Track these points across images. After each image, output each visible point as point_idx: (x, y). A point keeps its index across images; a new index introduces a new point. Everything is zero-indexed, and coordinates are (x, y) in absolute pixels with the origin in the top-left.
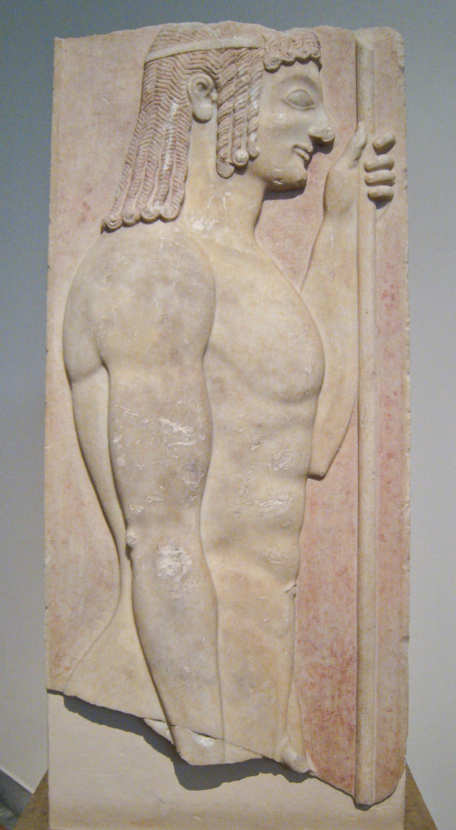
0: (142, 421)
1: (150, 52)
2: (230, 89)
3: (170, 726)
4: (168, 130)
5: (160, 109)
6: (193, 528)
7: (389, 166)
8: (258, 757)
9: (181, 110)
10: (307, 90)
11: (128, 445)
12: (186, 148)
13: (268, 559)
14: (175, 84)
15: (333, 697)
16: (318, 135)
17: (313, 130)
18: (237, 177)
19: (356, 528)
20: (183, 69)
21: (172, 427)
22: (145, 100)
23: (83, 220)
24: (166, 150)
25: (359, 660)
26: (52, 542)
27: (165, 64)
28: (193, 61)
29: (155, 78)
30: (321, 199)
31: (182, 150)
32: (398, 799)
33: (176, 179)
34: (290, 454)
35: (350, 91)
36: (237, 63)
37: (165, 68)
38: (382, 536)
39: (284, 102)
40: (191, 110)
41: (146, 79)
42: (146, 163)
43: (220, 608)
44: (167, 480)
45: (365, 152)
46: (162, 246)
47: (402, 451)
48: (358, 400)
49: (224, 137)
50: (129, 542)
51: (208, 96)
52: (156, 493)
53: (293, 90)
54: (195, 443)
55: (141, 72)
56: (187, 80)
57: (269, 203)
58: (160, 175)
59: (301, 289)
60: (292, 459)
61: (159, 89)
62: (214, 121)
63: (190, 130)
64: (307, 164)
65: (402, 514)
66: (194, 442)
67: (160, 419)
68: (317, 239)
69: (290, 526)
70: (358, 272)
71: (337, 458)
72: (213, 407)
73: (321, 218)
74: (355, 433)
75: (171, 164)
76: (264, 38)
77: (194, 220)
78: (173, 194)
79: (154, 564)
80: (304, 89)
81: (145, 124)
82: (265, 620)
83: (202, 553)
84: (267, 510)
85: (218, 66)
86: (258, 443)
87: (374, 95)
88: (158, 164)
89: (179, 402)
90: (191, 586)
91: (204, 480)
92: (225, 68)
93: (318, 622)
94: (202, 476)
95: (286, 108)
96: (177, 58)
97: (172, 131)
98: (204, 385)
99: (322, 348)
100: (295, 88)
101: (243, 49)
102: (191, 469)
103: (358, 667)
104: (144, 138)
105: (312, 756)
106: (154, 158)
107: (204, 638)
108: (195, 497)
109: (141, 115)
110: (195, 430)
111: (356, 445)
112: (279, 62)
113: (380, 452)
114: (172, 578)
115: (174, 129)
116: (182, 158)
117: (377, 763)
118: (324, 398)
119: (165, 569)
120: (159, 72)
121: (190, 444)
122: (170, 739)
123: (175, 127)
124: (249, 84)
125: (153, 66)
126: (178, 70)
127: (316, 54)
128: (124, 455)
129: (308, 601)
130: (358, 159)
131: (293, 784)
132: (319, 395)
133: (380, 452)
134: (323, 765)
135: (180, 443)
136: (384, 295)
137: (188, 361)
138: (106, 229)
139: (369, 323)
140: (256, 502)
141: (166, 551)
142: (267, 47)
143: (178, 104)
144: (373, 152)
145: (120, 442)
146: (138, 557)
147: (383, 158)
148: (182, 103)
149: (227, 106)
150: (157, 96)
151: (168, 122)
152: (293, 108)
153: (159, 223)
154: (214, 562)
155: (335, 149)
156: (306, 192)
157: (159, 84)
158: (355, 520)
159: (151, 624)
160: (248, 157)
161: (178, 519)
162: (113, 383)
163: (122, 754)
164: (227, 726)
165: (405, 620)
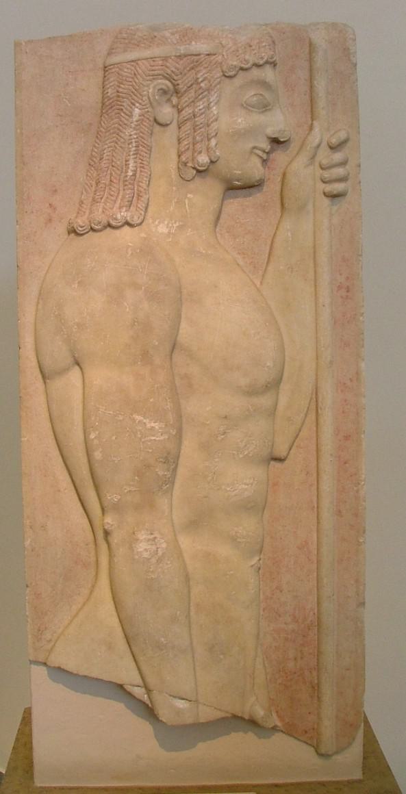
0: (116, 418)
1: (109, 54)
3: (149, 691)
4: (131, 135)
5: (123, 114)
6: (166, 514)
7: (343, 163)
8: (229, 715)
9: (143, 115)
17: (270, 131)
18: (198, 181)
19: (316, 506)
20: (144, 76)
21: (145, 423)
22: (107, 104)
24: (129, 155)
26: (31, 527)
27: (126, 70)
28: (154, 68)
32: (356, 749)
33: (141, 184)
34: (254, 442)
36: (197, 69)
38: (340, 512)
41: (107, 83)
42: (111, 167)
43: (191, 583)
46: (130, 253)
48: (317, 389)
50: (106, 527)
51: (169, 100)
52: (131, 483)
53: (250, 95)
54: (167, 437)
55: (101, 73)
56: (148, 86)
59: (261, 283)
61: (121, 94)
62: (174, 126)
63: (151, 134)
64: (264, 161)
65: (357, 491)
73: (279, 214)
75: (135, 168)
77: (159, 223)
78: (138, 199)
79: (131, 548)
80: (261, 93)
81: (107, 128)
86: (224, 433)
88: (122, 168)
89: (151, 400)
91: (175, 470)
92: (185, 74)
93: (281, 591)
94: (173, 467)
96: (137, 64)
97: (135, 137)
101: (202, 56)
102: (164, 461)
103: (318, 631)
104: (107, 142)
105: (277, 712)
107: (178, 613)
110: (166, 425)
111: (315, 429)
112: (237, 69)
113: (337, 435)
114: (148, 559)
115: (136, 134)
116: (145, 162)
117: (337, 717)
118: (285, 387)
119: (141, 552)
121: (162, 438)
122: (148, 702)
124: (209, 90)
125: (113, 70)
126: (139, 76)
128: (101, 450)
130: (313, 157)
136: (340, 288)
138: (73, 231)
139: (326, 314)
140: (223, 487)
141: (142, 536)
142: (224, 53)
143: (140, 109)
144: (329, 150)
145: (95, 438)
147: (338, 157)
149: (187, 112)
153: (126, 228)
154: (185, 542)
157: (121, 90)
158: (315, 499)
160: (209, 161)
162: (86, 381)
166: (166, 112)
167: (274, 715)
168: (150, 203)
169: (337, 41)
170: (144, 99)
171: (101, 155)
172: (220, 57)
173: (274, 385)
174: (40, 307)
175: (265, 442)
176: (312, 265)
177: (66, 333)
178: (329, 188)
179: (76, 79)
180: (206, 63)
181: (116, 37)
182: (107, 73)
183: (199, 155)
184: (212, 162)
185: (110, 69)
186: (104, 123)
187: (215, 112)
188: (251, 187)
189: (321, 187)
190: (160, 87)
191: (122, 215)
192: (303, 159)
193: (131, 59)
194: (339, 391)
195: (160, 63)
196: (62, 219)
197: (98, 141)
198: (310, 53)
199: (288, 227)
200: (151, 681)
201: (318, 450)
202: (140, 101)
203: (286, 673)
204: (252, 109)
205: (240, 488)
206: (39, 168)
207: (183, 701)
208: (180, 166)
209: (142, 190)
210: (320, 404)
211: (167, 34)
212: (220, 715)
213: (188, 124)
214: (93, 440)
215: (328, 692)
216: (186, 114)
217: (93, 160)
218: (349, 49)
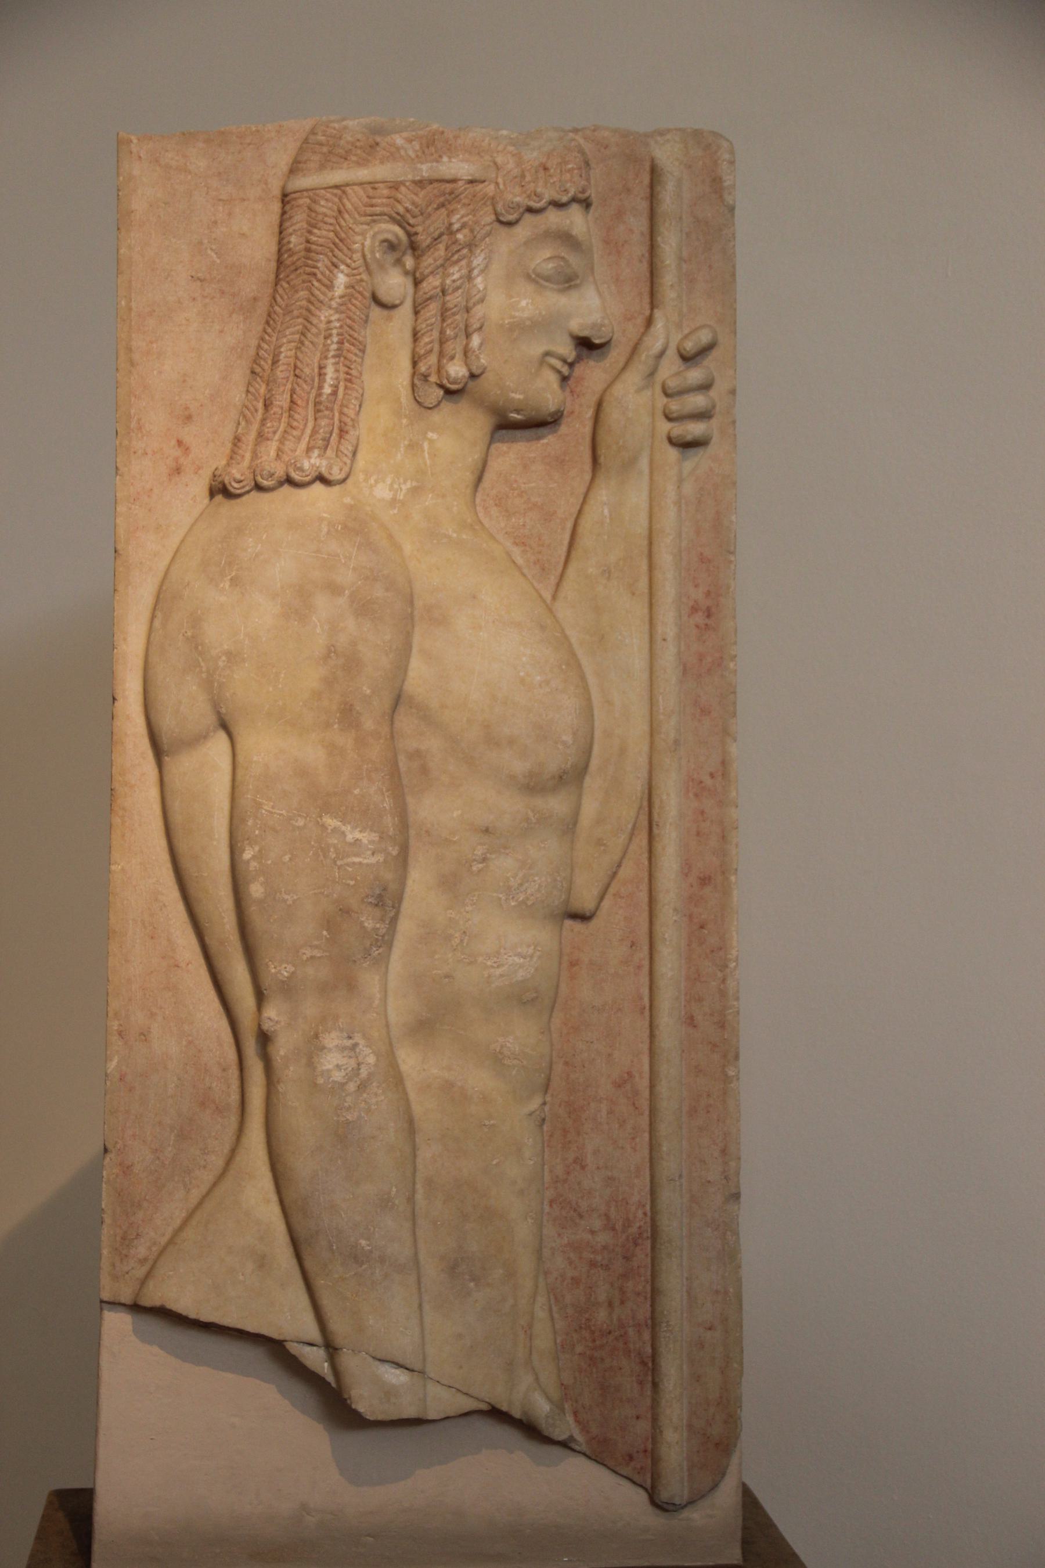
3: (331, 1348)
4: (329, 322)
5: (316, 283)
6: (377, 1002)
7: (705, 387)
8: (484, 1407)
9: (353, 287)
10: (566, 256)
11: (269, 862)
12: (360, 354)
13: (500, 1056)
14: (341, 240)
15: (610, 1304)
16: (583, 334)
17: (577, 325)
18: (447, 407)
19: (647, 1005)
20: (357, 216)
22: (288, 262)
23: (178, 470)
24: (326, 358)
26: (120, 1033)
27: (323, 203)
28: (374, 201)
31: (354, 358)
33: (345, 410)
35: (638, 249)
36: (451, 208)
37: (324, 210)
38: (692, 1018)
39: (528, 277)
42: (291, 378)
44: (336, 920)
46: (325, 530)
47: (723, 873)
49: (426, 339)
52: (316, 943)
53: (543, 259)
54: (382, 860)
55: (276, 207)
56: (363, 234)
58: (316, 404)
59: (554, 597)
60: (540, 885)
62: (407, 308)
63: (366, 322)
65: (724, 981)
66: (380, 858)
67: (324, 819)
68: (580, 512)
71: (613, 885)
72: (409, 799)
73: (588, 477)
74: (645, 842)
75: (336, 382)
76: (495, 163)
77: (376, 482)
78: (341, 437)
79: (311, 1064)
81: (287, 306)
82: (494, 1162)
84: (498, 972)
85: (416, 211)
86: (484, 860)
87: (680, 259)
88: (313, 381)
89: (357, 792)
90: (374, 1100)
91: (394, 920)
92: (430, 215)
93: (583, 1168)
94: (392, 914)
95: (530, 288)
96: (344, 192)
97: (338, 325)
98: (395, 764)
99: (589, 700)
100: (548, 253)
101: (460, 183)
103: (653, 1248)
105: (575, 1414)
106: (307, 371)
107: (394, 1189)
108: (381, 950)
109: (280, 291)
111: (646, 863)
112: (521, 210)
113: (686, 875)
114: (343, 1085)
115: (339, 320)
116: (354, 372)
117: (690, 1427)
118: (593, 783)
119: (329, 1071)
120: (313, 215)
121: (373, 860)
122: (330, 1378)
123: (343, 316)
124: (471, 246)
125: (301, 202)
126: (346, 216)
127: (583, 191)
129: (565, 1132)
130: (652, 374)
132: (583, 778)
133: (686, 875)
135: (357, 860)
136: (694, 610)
138: (220, 490)
139: (668, 657)
140: (480, 959)
141: (332, 1040)
142: (500, 180)
143: (347, 275)
144: (678, 361)
145: (254, 857)
146: (282, 1053)
147: (695, 375)
148: (354, 275)
149: (431, 284)
151: (330, 307)
153: (318, 488)
156: (563, 429)
157: (314, 239)
159: (303, 1166)
160: (467, 374)
161: (351, 986)
162: (240, 758)
165: (733, 1164)
166: (394, 283)
167: (570, 1419)
168: (360, 447)
169: (701, 163)
172: (492, 187)
173: (572, 777)
174: (157, 623)
175: (555, 880)
176: (644, 567)
178: (679, 430)
179: (230, 214)
181: (306, 141)
182: (287, 207)
183: (450, 363)
184: (473, 376)
185: (295, 199)
186: (282, 297)
187: (481, 287)
188: (539, 424)
189: (664, 427)
190: (381, 237)
191: (313, 463)
193: (332, 183)
194: (691, 795)
195: (386, 192)
196: (199, 468)
197: (269, 330)
198: (652, 186)
199: (605, 498)
200: (339, 1326)
202: (349, 261)
203: (593, 1332)
204: (547, 284)
206: (160, 373)
207: (398, 1372)
208: (416, 381)
209: (348, 420)
211: (399, 141)
213: (431, 307)
214: (248, 862)
215: (673, 1370)
217: (259, 365)
218: (720, 179)
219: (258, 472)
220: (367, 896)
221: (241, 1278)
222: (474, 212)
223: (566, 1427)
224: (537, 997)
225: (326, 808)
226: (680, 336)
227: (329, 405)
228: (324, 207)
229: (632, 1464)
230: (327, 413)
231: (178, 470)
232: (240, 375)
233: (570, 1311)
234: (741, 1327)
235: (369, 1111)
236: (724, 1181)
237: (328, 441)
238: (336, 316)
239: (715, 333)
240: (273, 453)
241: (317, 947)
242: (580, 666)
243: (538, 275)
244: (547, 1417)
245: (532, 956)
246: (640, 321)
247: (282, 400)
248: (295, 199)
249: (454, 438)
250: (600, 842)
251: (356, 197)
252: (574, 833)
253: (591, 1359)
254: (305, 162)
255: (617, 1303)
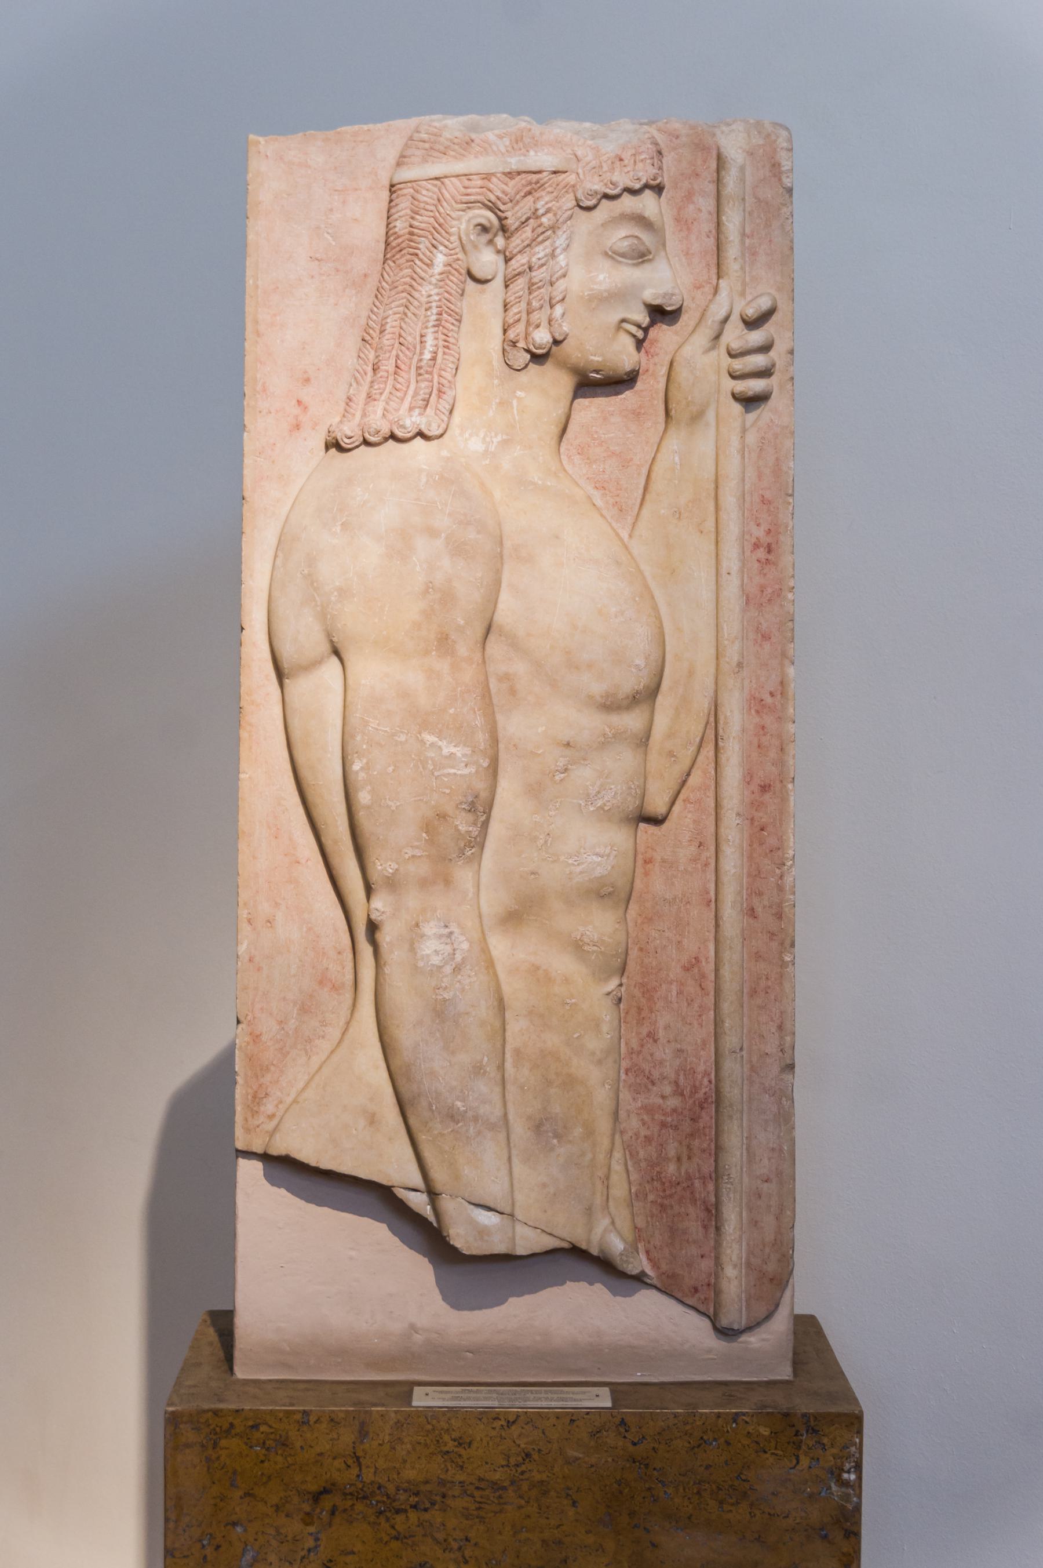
0: (396, 738)
2: (524, 236)
3: (433, 1194)
4: (430, 296)
5: (417, 262)
8: (566, 1245)
9: (450, 265)
10: (640, 236)
14: (440, 225)
15: (679, 1159)
16: (657, 302)
17: (651, 295)
21: (440, 748)
22: (394, 244)
24: (427, 328)
25: (718, 1102)
26: (249, 921)
27: (424, 192)
29: (408, 211)
30: (662, 395)
31: (452, 327)
35: (706, 225)
36: (537, 195)
37: (425, 199)
38: (753, 909)
39: (606, 254)
40: (465, 266)
42: (397, 345)
43: (508, 1015)
44: (432, 825)
45: (728, 326)
46: (424, 479)
49: (515, 310)
51: (491, 242)
53: (620, 237)
54: (473, 771)
55: (386, 194)
56: (459, 219)
57: (581, 402)
58: (418, 368)
59: (630, 536)
60: (616, 793)
62: (498, 283)
63: (462, 295)
64: (639, 344)
65: (781, 877)
67: (423, 735)
68: (654, 459)
69: (613, 893)
70: (717, 508)
71: (683, 791)
72: (500, 718)
74: (712, 753)
77: (471, 435)
78: (439, 397)
79: (412, 949)
81: (393, 282)
82: (575, 1036)
83: (483, 932)
84: (579, 869)
85: (506, 199)
86: (566, 770)
87: (743, 235)
89: (452, 711)
90: (468, 981)
91: (486, 824)
92: (518, 202)
93: (655, 1041)
94: (484, 818)
95: (607, 264)
96: (443, 183)
97: (437, 298)
99: (661, 627)
100: (623, 233)
101: (545, 174)
103: (717, 1111)
104: (393, 305)
105: (647, 1252)
106: (409, 338)
107: (486, 1059)
108: (473, 850)
109: (387, 268)
110: (473, 751)
111: (713, 772)
112: (599, 197)
113: (748, 783)
114: (441, 967)
115: (438, 294)
116: (451, 340)
117: (748, 1264)
119: (428, 956)
120: (416, 203)
121: (466, 771)
122: (432, 1218)
123: (442, 290)
124: (553, 228)
125: (405, 191)
126: (445, 204)
127: (654, 179)
128: (369, 788)
129: (640, 1010)
130: (717, 337)
131: (619, 1299)
132: (656, 696)
133: (748, 783)
134: (664, 1267)
135: (452, 771)
136: (756, 546)
137: (462, 650)
138: (335, 445)
139: (732, 588)
140: (562, 858)
141: (430, 929)
142: (580, 171)
144: (741, 325)
145: (362, 768)
146: (388, 939)
147: (756, 337)
149: (519, 262)
150: (411, 241)
151: (430, 283)
152: (620, 262)
154: (500, 946)
155: (684, 318)
156: (639, 385)
157: (416, 223)
158: (712, 886)
159: (406, 1037)
160: (551, 340)
161: (447, 881)
162: (350, 681)
163: (353, 1253)
164: (519, 1197)
165: (788, 1039)
166: (486, 261)
167: (643, 1257)
168: (456, 405)
170: (452, 239)
171: (382, 325)
172: (573, 176)
173: (648, 695)
174: (279, 562)
175: (630, 788)
177: (319, 603)
178: (740, 386)
179: (344, 202)
180: (550, 186)
181: (411, 139)
182: (394, 195)
184: (556, 342)
185: (400, 189)
187: (563, 264)
188: (618, 382)
189: (732, 383)
191: (412, 421)
192: (701, 339)
194: (753, 712)
195: (480, 183)
196: (316, 424)
197: (377, 303)
198: (718, 171)
199: (675, 447)
200: (440, 1176)
201: (717, 806)
202: (447, 243)
203: (664, 1184)
205: (589, 859)
206: (282, 341)
207: (490, 1214)
208: (506, 347)
210: (721, 732)
211: (491, 136)
212: (551, 1243)
213: (519, 281)
214: (357, 772)
215: (732, 1217)
216: (518, 265)
217: (368, 334)
218: (779, 165)
219: (365, 430)
220: (461, 803)
221: (354, 1132)
222: (557, 198)
223: (641, 1263)
224: (614, 892)
225: (425, 725)
226: (743, 303)
227: (429, 369)
228: (427, 196)
229: (697, 1295)
230: (427, 376)
231: (298, 427)
232: (352, 342)
233: (643, 1164)
234: (794, 1180)
235: (463, 990)
236: (780, 1054)
237: (428, 401)
238: (436, 291)
239: (775, 300)
240: (380, 412)
241: (417, 847)
242: (653, 598)
243: (614, 253)
244: (621, 1254)
245: (608, 856)
246: (708, 289)
247: (388, 366)
248: (400, 189)
249: (545, 391)
250: (671, 754)
251: (453, 187)
252: (647, 746)
253: (662, 1205)
254: (409, 157)
255: (685, 1158)
